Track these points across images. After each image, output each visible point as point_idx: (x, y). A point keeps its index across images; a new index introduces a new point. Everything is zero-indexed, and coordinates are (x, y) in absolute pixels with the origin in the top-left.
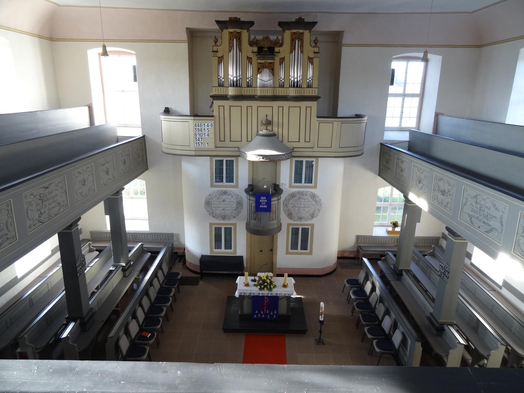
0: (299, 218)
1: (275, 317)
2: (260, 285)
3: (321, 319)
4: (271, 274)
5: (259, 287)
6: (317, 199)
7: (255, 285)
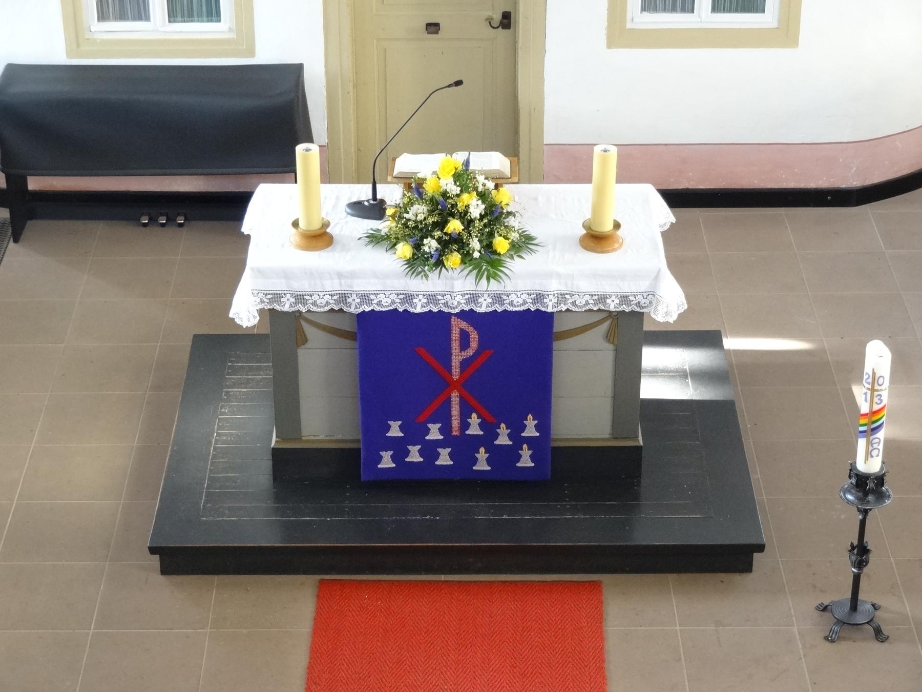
1: (526, 460)
2: (416, 233)
3: (869, 463)
4: (490, 161)
5: (405, 249)
7: (375, 239)
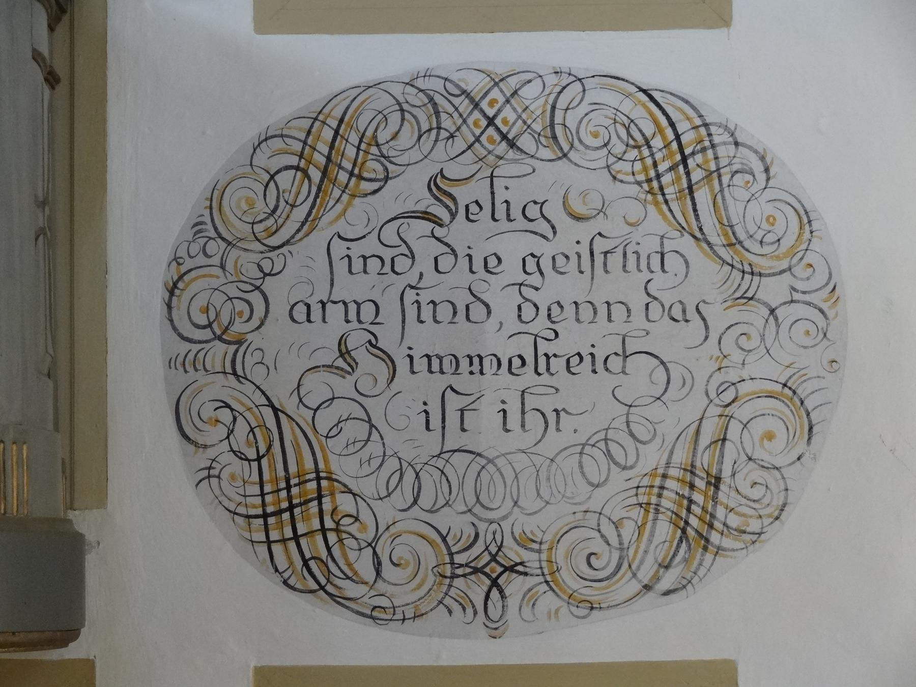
0: (451, 571)
6: (749, 209)
